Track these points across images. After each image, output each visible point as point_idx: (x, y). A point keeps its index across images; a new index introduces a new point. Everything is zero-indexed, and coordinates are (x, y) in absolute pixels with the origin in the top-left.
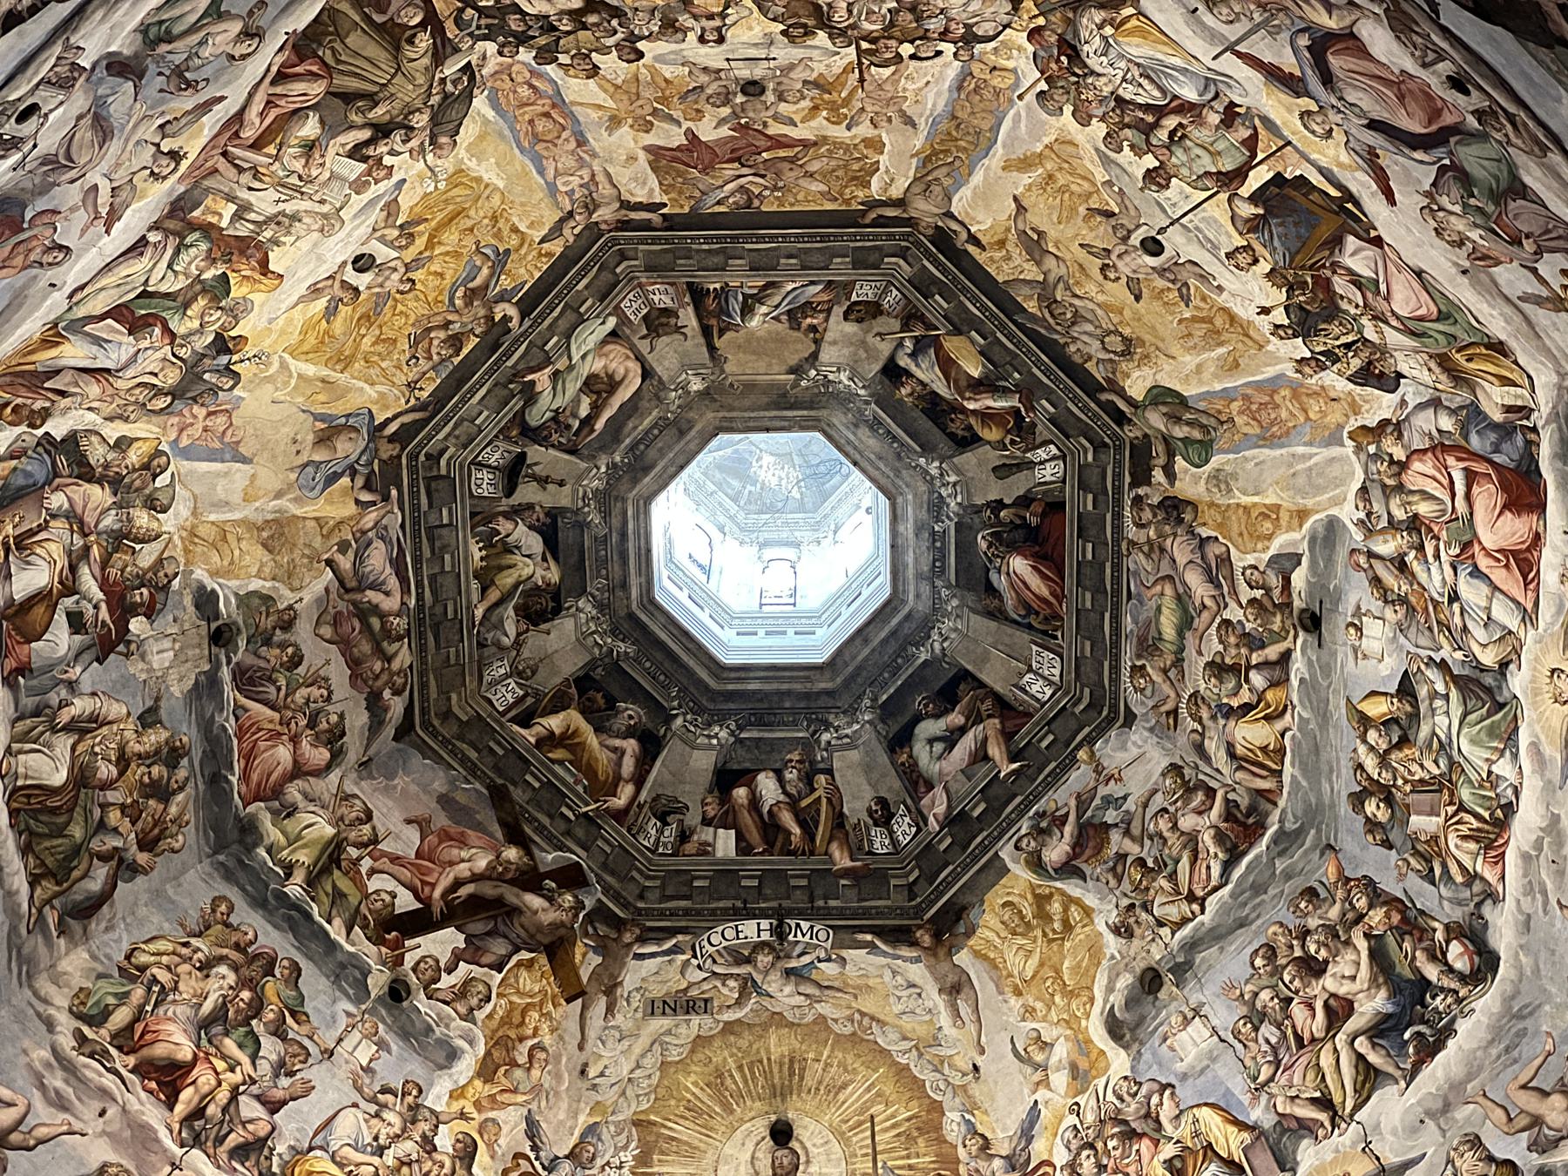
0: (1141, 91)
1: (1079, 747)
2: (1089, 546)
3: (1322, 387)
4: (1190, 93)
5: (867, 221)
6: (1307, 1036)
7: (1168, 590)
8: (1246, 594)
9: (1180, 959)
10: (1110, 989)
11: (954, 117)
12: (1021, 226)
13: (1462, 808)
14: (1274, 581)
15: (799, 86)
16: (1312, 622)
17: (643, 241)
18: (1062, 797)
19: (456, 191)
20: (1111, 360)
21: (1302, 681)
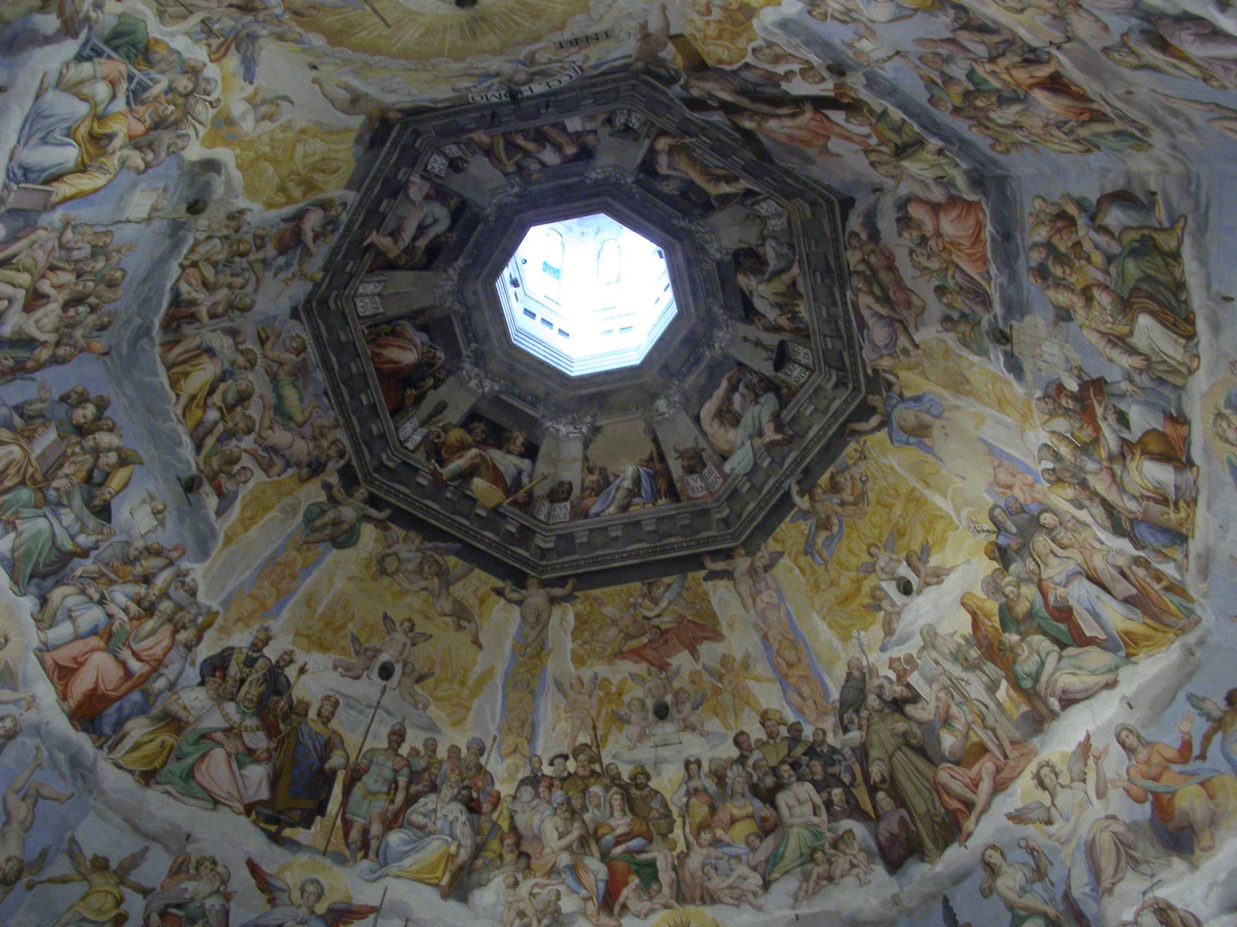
0: (422, 810)
1: (323, 279)
2: (365, 402)
3: (248, 626)
4: (395, 838)
5: (571, 583)
6: (50, 274)
7: (299, 418)
8: (246, 461)
9: (181, 234)
10: (228, 183)
11: (532, 693)
12: (473, 625)
13: (22, 483)
14: (228, 485)
15: (634, 718)
16: (190, 486)
17: (714, 540)
18: (321, 252)
19: (845, 623)
20: (389, 546)
21: (180, 444)
